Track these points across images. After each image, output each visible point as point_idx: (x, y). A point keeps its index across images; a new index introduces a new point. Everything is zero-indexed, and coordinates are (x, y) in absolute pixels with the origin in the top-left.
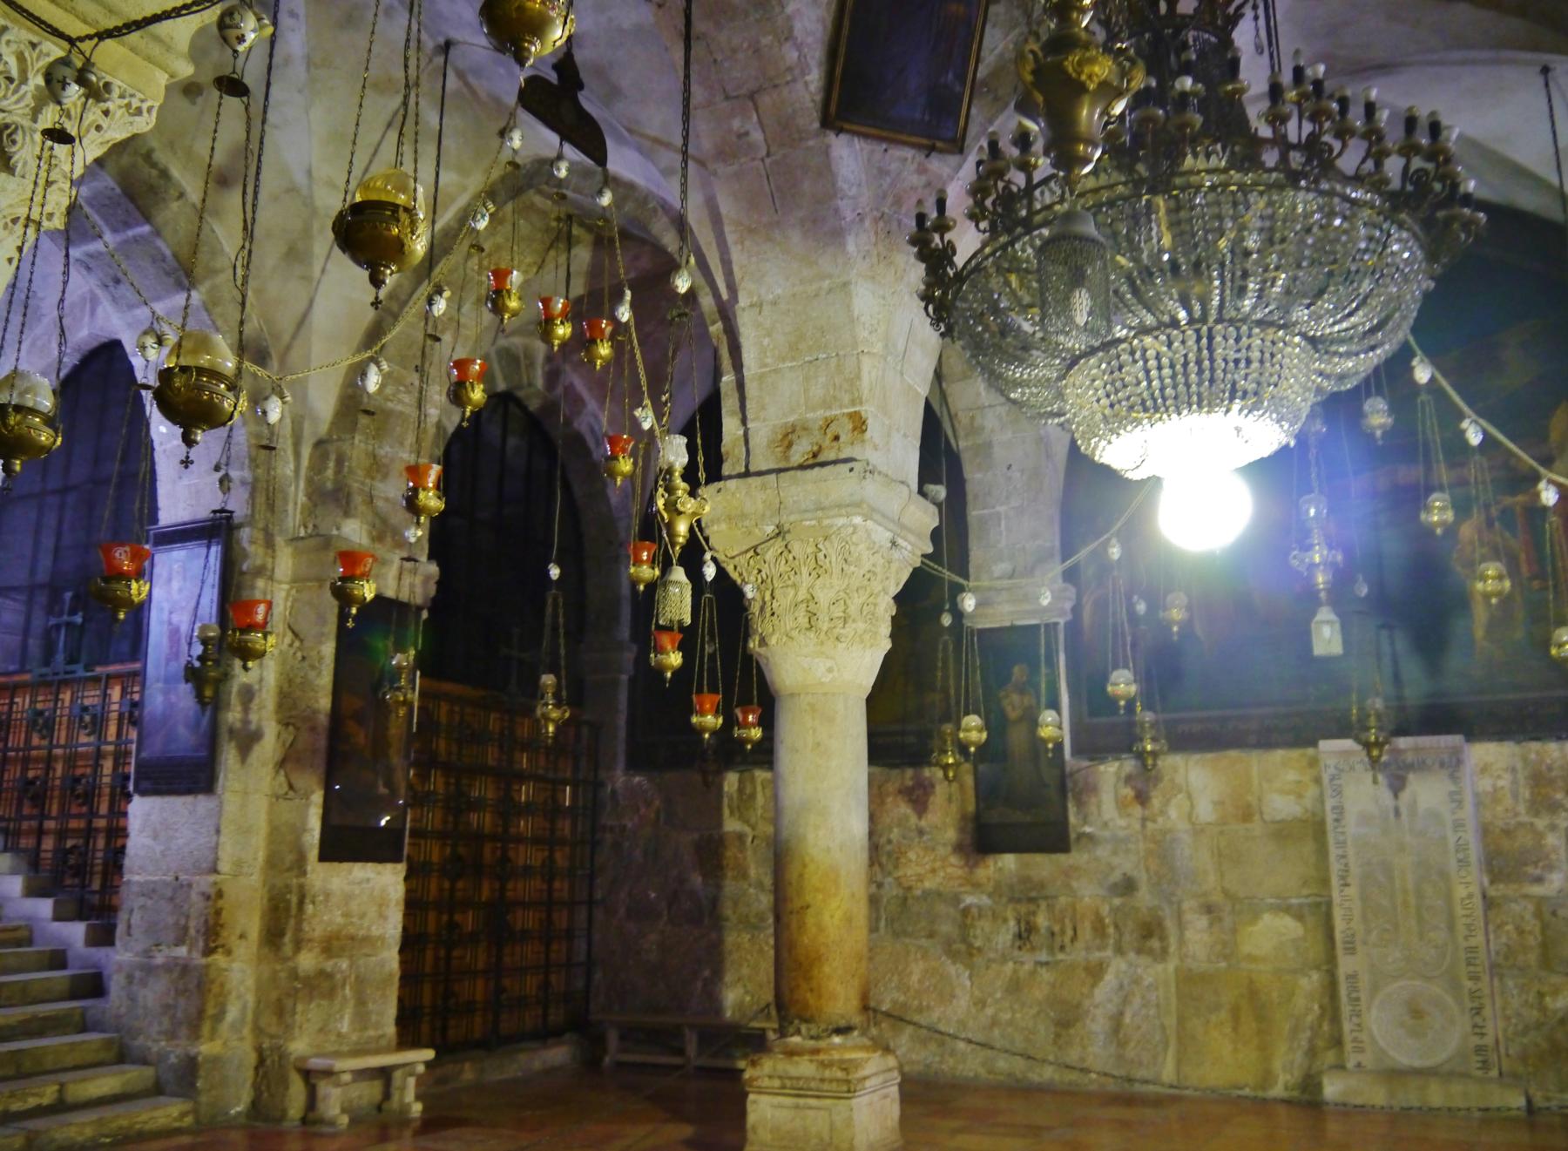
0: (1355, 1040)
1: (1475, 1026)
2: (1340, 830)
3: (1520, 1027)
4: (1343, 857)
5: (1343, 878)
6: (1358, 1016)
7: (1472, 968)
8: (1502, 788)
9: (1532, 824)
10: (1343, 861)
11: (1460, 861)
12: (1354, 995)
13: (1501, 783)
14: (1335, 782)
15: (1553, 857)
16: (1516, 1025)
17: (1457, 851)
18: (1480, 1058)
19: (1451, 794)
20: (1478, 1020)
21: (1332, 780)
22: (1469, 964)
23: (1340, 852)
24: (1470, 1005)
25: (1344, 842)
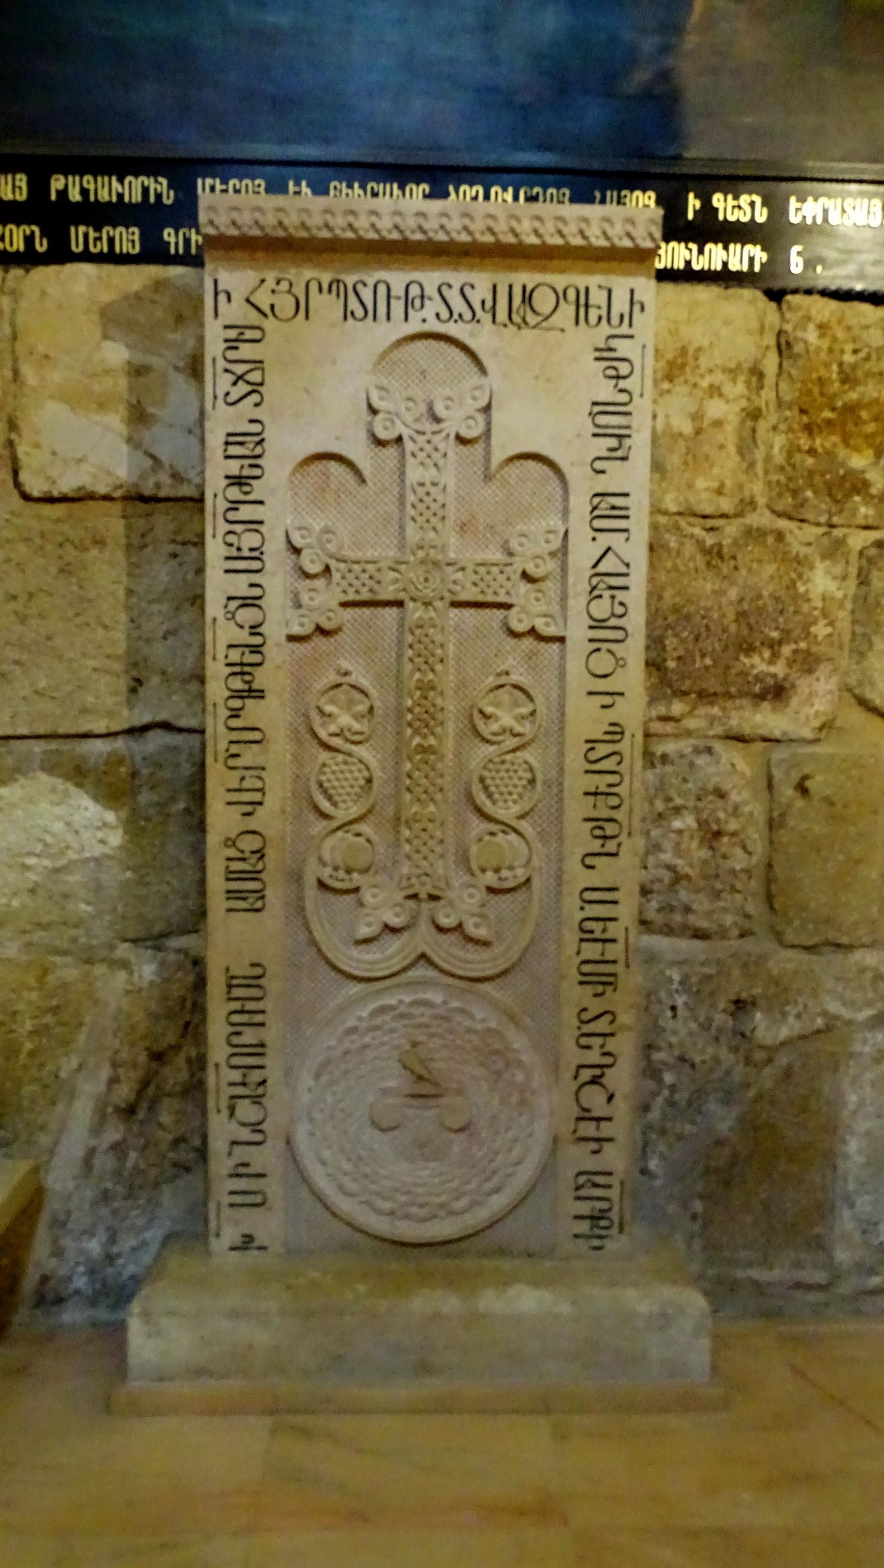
0: (240, 1171)
1: (585, 1115)
2: (246, 512)
3: (682, 1097)
4: (249, 602)
5: (241, 669)
6: (257, 1100)
7: (591, 951)
8: (718, 424)
9: (780, 536)
10: (247, 616)
11: (598, 624)
12: (249, 1036)
13: (715, 408)
14: (246, 351)
15: (821, 630)
16: (673, 1088)
17: (594, 594)
18: (584, 1208)
19: (600, 408)
20: (595, 1099)
21: (232, 344)
22: (587, 936)
23: (240, 585)
24: (573, 1056)
25: (257, 554)
